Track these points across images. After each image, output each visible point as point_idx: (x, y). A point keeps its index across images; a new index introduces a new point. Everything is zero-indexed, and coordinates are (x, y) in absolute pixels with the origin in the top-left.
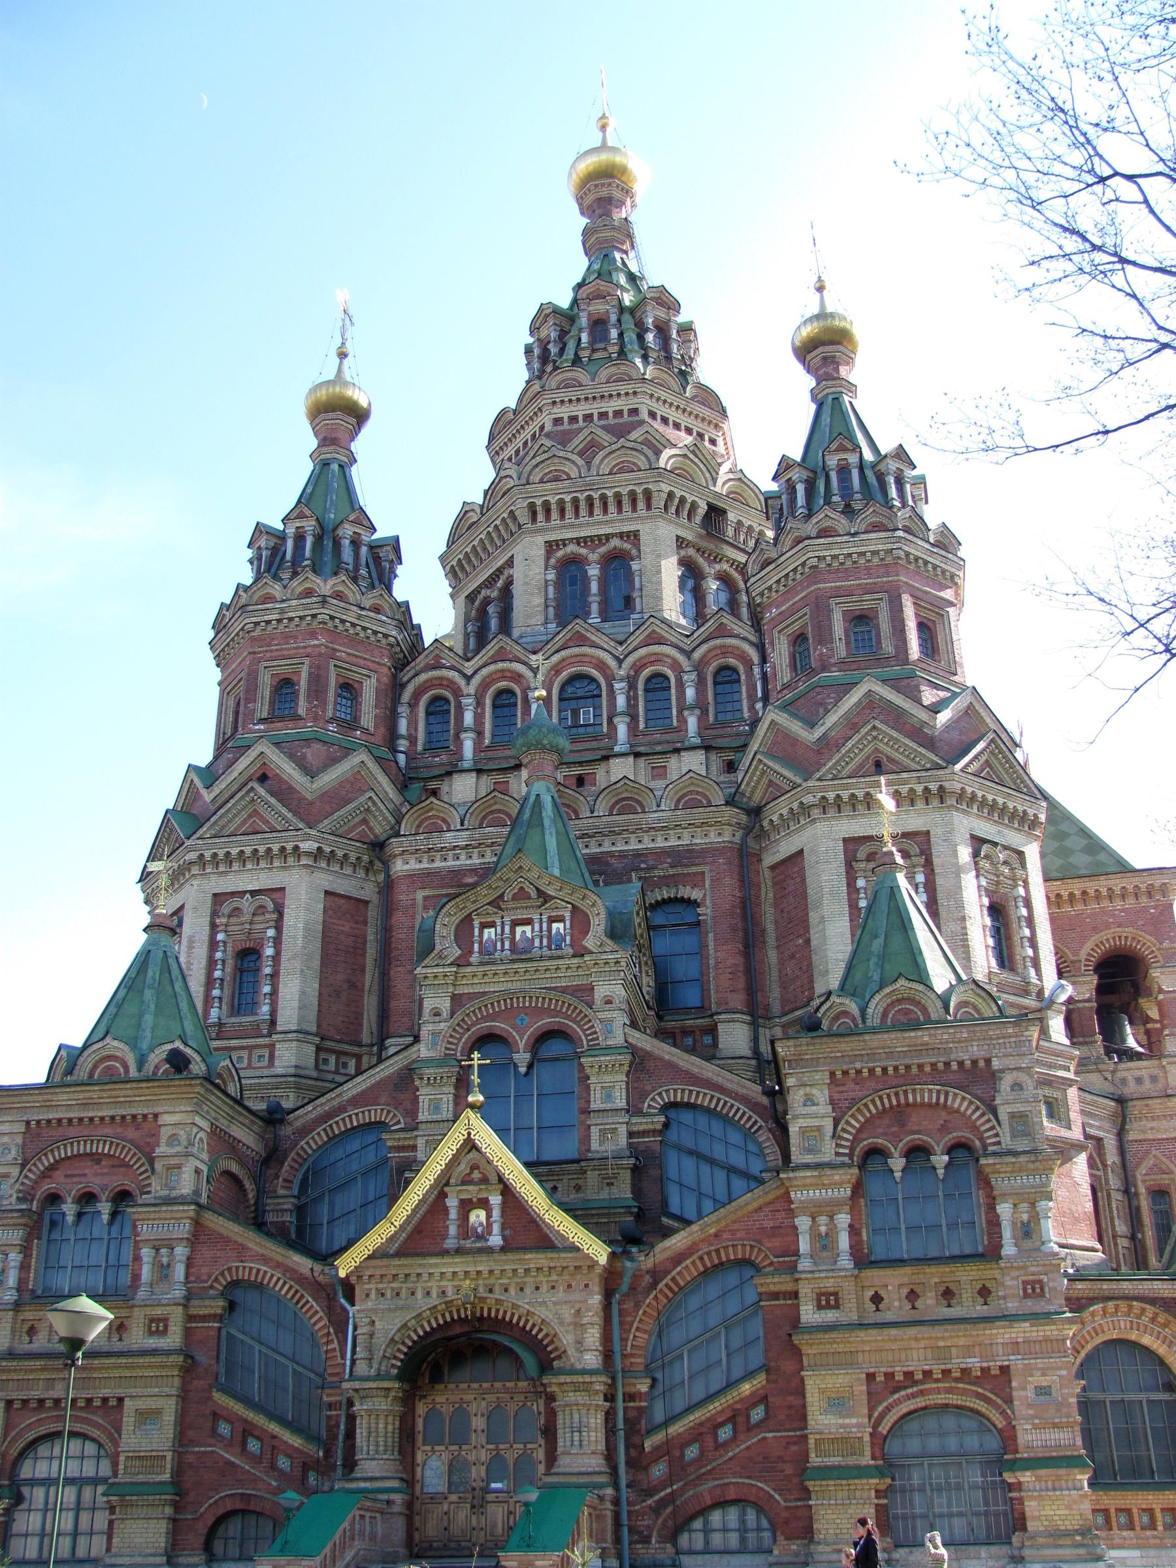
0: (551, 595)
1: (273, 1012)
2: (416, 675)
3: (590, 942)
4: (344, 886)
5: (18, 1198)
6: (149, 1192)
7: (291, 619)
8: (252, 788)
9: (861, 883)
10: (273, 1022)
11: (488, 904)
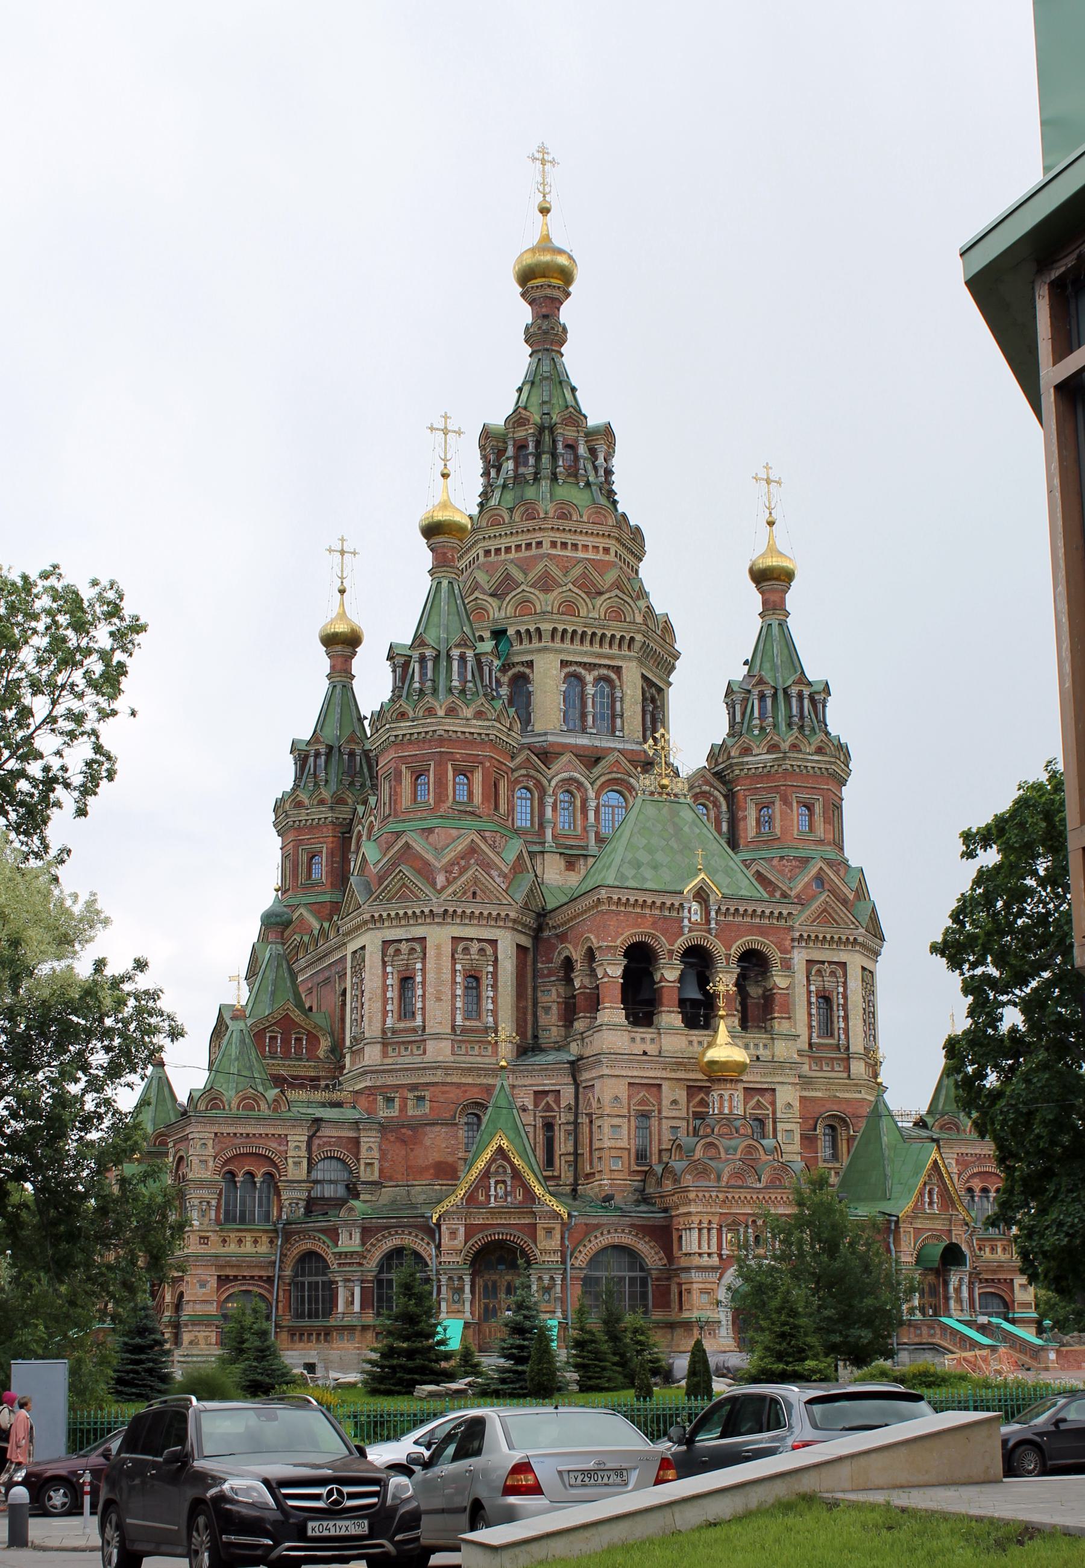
9: (813, 988)
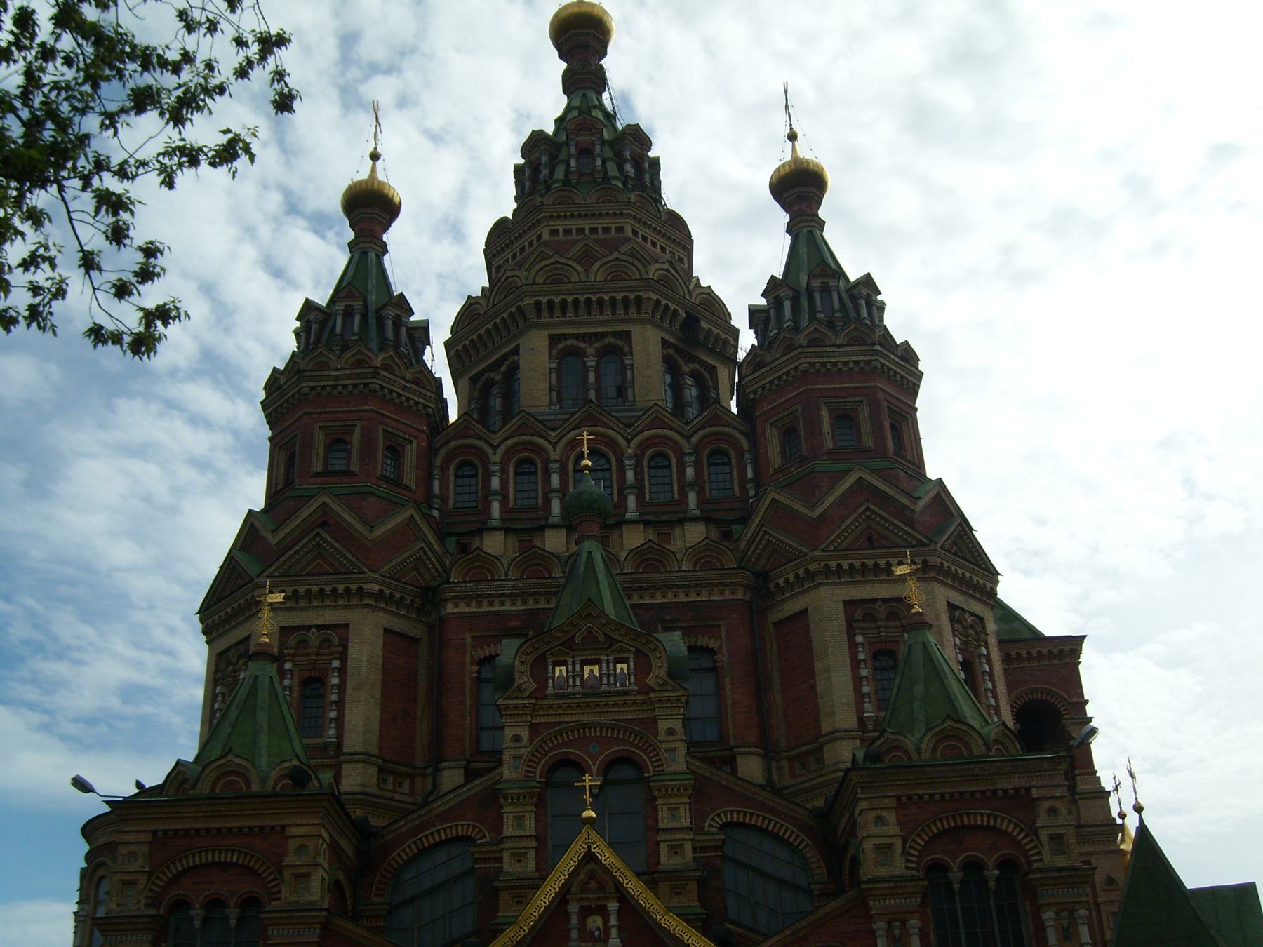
0: (554, 381)
1: (340, 736)
2: (448, 442)
3: (650, 681)
4: (398, 625)
5: (146, 904)
6: (279, 899)
7: (345, 386)
8: (318, 534)
9: (859, 639)
10: (339, 745)
11: (561, 644)
